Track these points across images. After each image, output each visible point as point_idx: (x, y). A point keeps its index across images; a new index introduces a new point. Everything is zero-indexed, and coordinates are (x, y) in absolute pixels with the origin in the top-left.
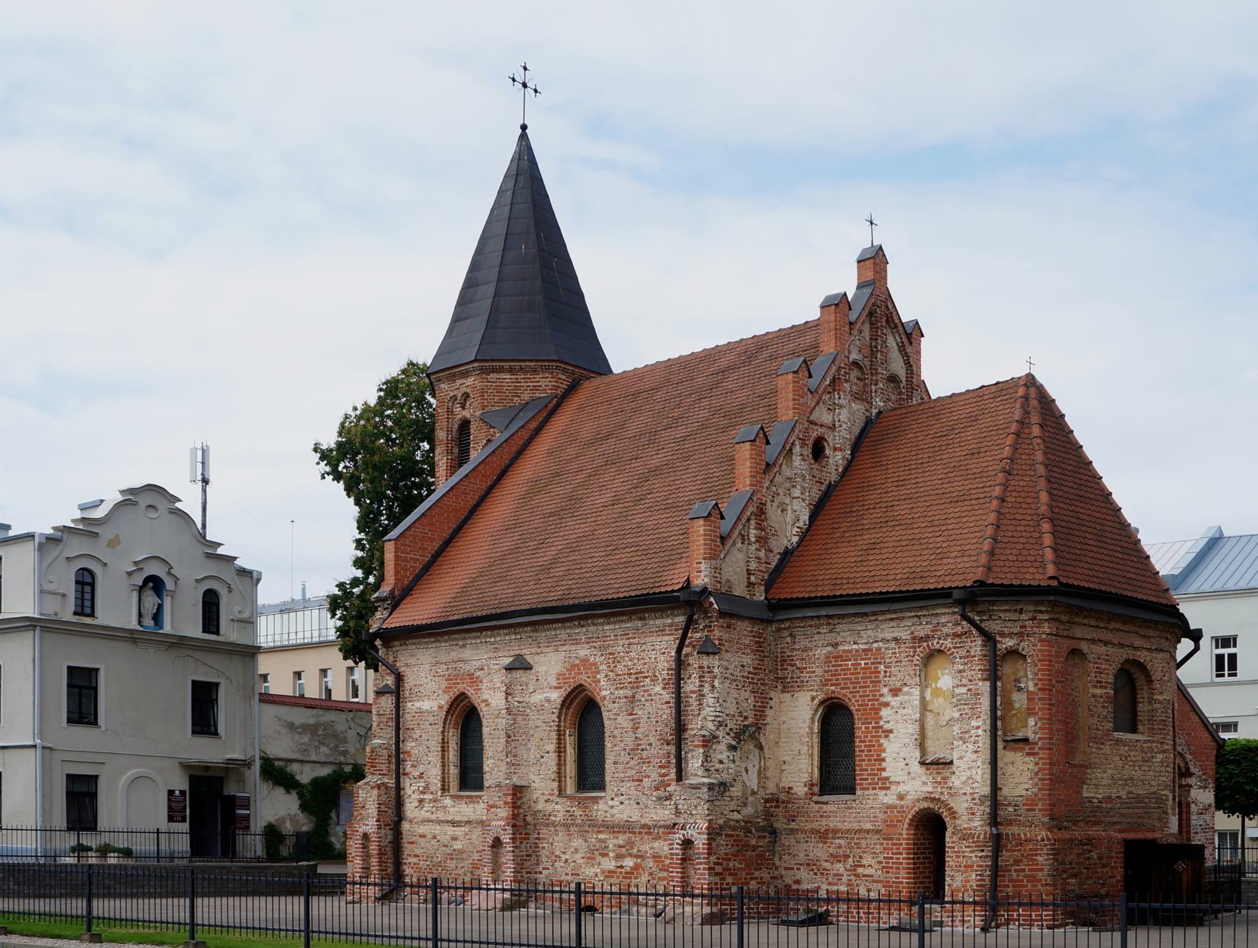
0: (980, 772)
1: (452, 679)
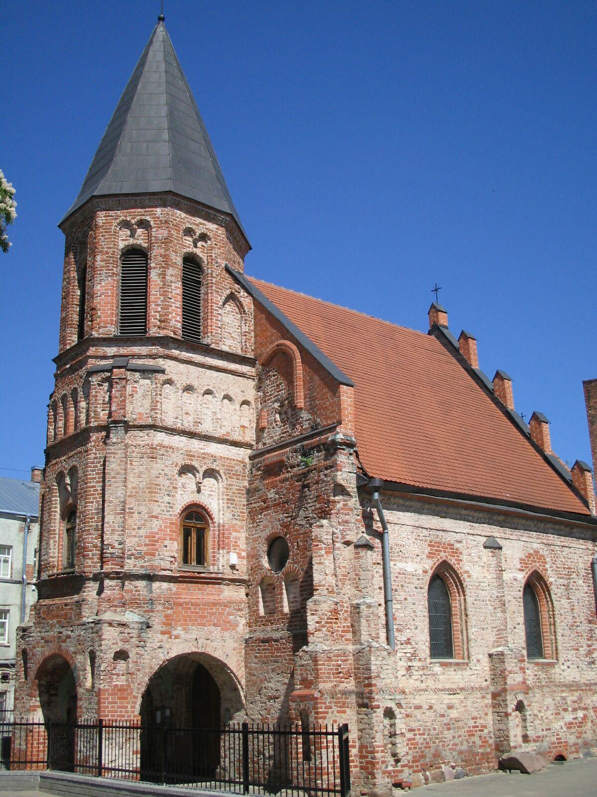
1: (435, 547)
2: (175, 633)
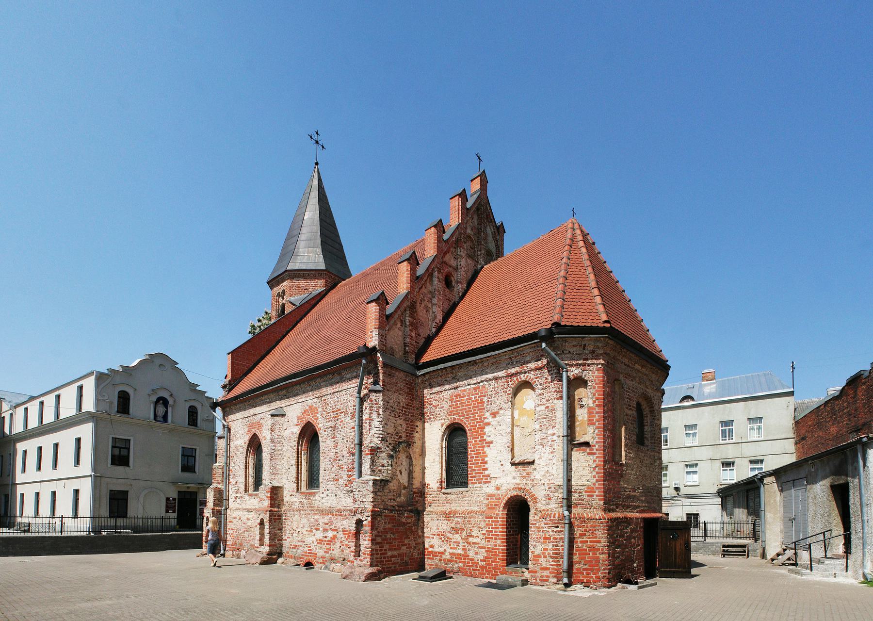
0: (555, 467)
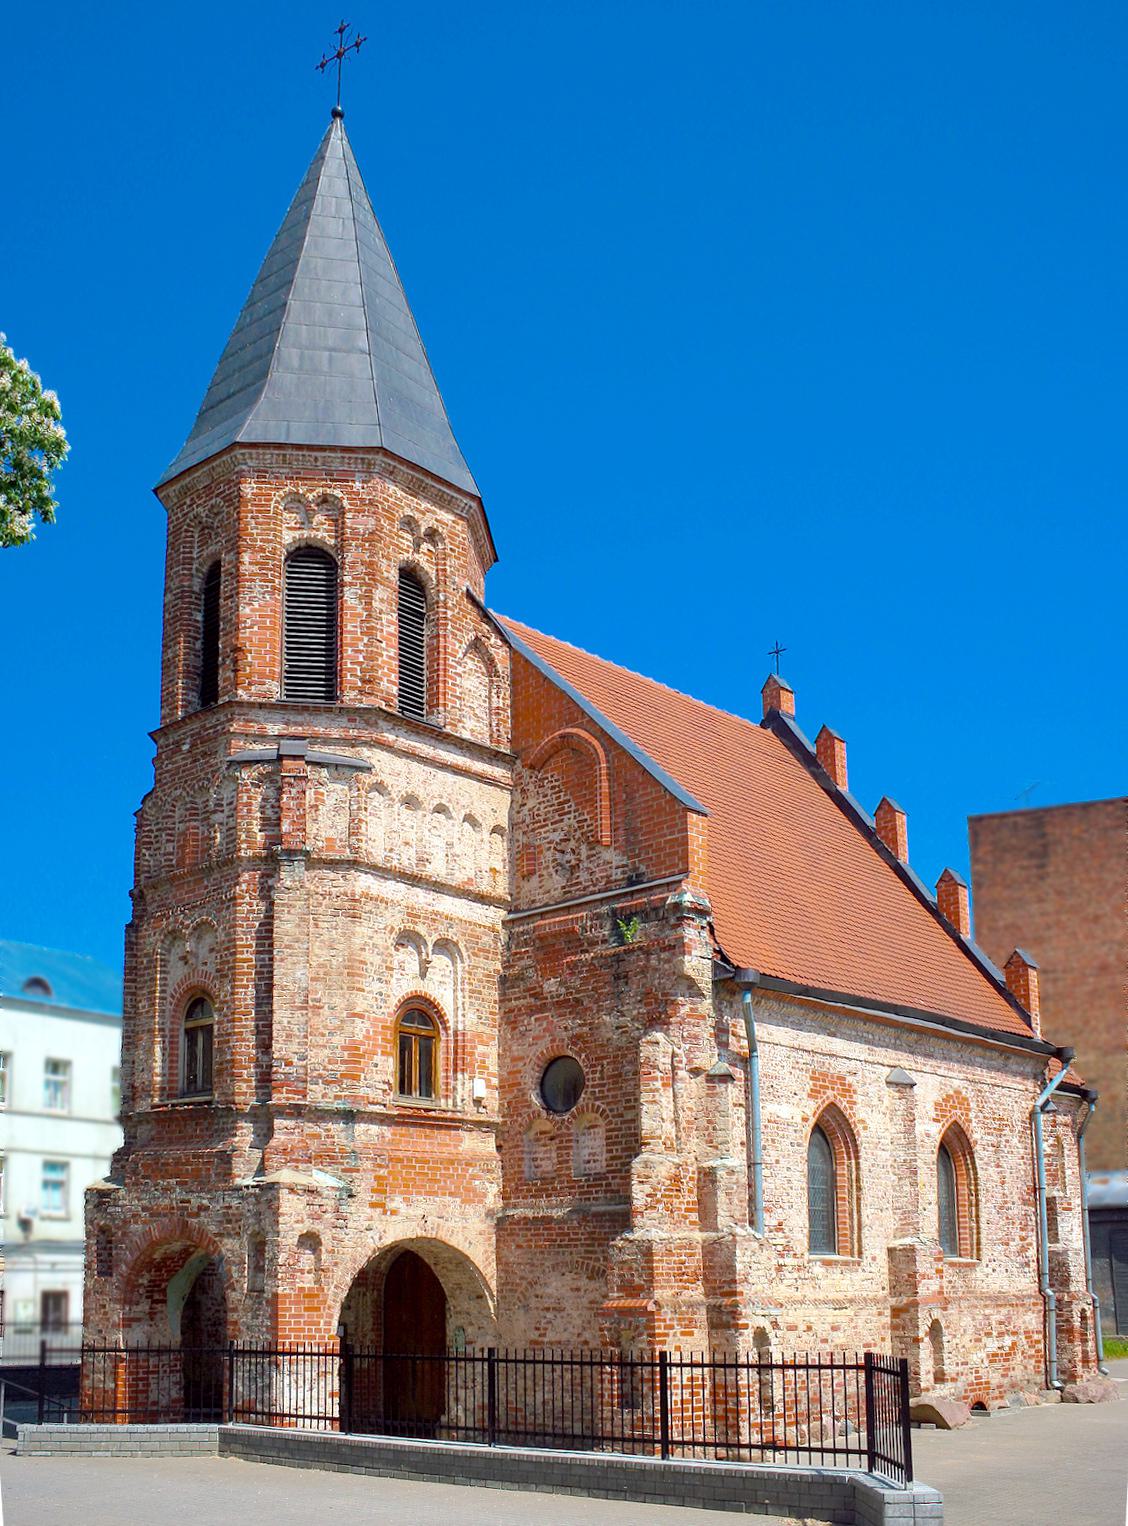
1: (821, 1081)
2: (391, 1206)
